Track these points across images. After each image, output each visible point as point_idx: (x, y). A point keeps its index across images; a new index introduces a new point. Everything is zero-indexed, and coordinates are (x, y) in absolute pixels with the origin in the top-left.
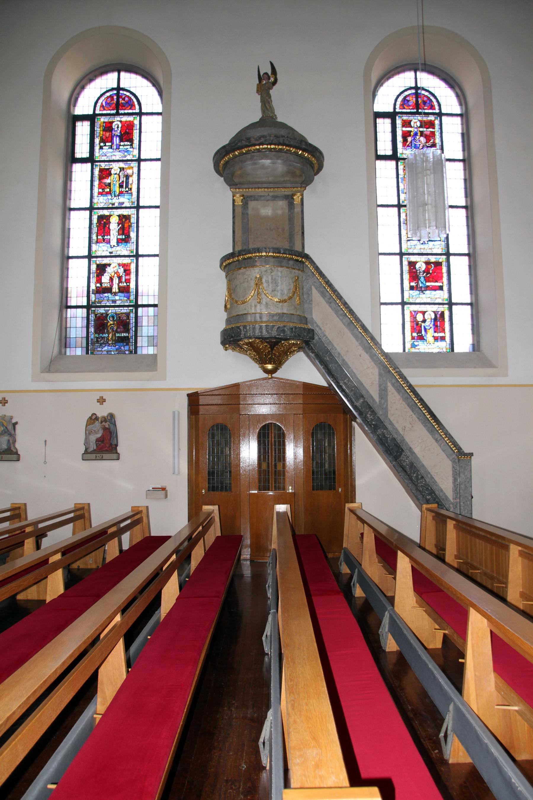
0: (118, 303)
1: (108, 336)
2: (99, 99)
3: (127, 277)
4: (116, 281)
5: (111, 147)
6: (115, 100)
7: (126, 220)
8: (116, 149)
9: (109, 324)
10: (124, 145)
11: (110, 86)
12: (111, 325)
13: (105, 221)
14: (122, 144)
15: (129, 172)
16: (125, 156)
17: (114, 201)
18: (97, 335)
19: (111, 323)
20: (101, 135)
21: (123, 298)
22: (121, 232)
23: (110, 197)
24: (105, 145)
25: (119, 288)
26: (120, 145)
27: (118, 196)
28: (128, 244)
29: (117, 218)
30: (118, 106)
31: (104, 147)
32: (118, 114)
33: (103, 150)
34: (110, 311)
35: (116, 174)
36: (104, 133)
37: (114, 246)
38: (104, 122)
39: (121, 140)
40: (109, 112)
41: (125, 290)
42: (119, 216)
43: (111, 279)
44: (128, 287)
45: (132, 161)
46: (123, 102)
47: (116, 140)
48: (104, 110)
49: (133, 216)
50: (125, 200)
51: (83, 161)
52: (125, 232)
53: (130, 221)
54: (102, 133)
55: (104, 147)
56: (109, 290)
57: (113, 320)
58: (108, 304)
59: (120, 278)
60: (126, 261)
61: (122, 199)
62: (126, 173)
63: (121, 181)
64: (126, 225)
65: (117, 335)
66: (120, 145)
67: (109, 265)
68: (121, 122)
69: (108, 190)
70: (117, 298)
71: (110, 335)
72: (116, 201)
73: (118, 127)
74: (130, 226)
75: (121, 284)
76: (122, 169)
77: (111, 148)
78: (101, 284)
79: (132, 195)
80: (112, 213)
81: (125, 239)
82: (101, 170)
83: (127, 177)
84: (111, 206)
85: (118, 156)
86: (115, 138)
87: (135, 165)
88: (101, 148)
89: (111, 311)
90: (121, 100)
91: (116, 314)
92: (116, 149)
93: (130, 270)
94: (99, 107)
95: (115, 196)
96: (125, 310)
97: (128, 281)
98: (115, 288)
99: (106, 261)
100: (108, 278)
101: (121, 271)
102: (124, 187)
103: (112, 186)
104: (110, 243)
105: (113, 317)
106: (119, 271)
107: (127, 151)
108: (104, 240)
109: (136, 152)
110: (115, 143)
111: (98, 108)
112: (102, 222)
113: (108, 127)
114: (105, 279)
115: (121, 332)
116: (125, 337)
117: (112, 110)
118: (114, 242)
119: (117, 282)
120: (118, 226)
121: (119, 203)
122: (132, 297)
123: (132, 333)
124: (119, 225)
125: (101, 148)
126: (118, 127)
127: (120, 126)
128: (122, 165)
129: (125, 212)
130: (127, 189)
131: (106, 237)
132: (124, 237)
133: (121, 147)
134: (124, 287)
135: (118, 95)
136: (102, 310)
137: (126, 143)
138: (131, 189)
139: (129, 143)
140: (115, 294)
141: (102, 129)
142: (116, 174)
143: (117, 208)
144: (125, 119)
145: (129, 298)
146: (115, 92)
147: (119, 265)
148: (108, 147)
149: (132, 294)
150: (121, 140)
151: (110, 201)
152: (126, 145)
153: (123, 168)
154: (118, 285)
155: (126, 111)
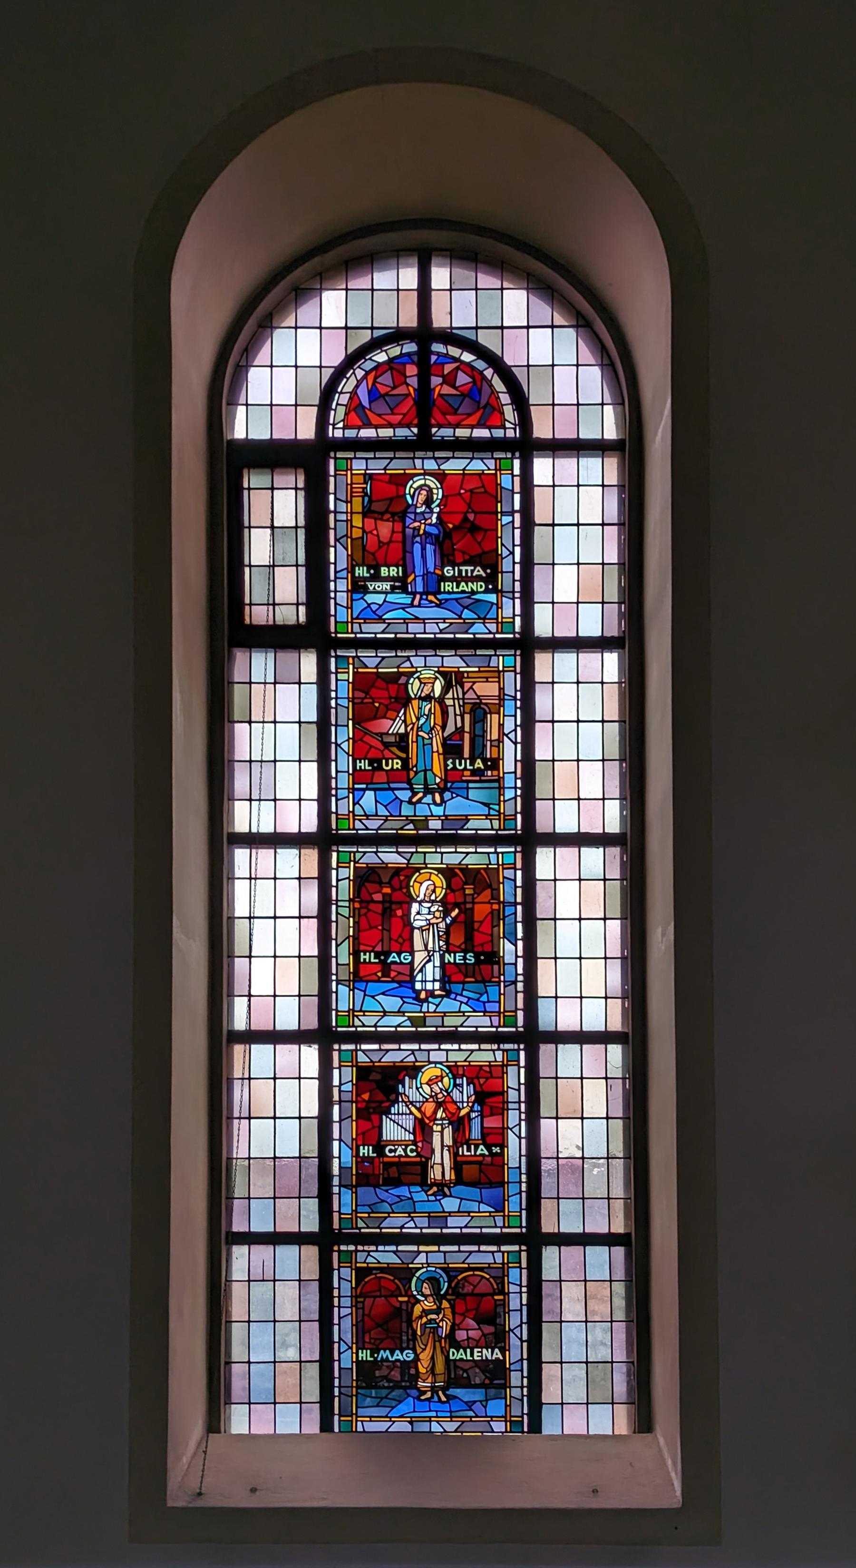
0: (455, 1225)
1: (417, 1359)
2: (340, 373)
3: (492, 1123)
4: (442, 1137)
5: (401, 585)
6: (414, 382)
7: (478, 892)
8: (426, 593)
9: (417, 1310)
10: (452, 579)
11: (386, 319)
12: (425, 1312)
13: (387, 890)
14: (448, 571)
15: (487, 689)
16: (468, 626)
17: (422, 810)
18: (365, 1355)
19: (429, 1304)
20: (357, 533)
21: (474, 1206)
22: (458, 939)
23: (404, 795)
24: (376, 577)
25: (457, 1166)
26: (443, 578)
27: (442, 791)
28: (492, 990)
29: (439, 881)
30: (425, 408)
31: (371, 586)
32: (424, 443)
33: (370, 598)
34: (422, 1258)
35: (428, 698)
36: (370, 522)
37: (431, 994)
38: (369, 477)
39: (446, 558)
40: (386, 433)
41: (482, 1174)
42: (448, 873)
43: (423, 1129)
44: (498, 1161)
45: (495, 644)
46: (447, 390)
47: (424, 558)
48: (368, 425)
49: (509, 873)
50: (470, 807)
51: (279, 638)
52: (478, 938)
53: (495, 897)
54: (358, 521)
55: (371, 586)
56: (414, 1171)
57: (437, 1296)
58: (410, 1229)
59: (459, 1124)
60: (485, 1055)
61: (456, 806)
62: (470, 695)
63: (450, 729)
64: (481, 911)
65: (456, 1355)
66: (443, 578)
67: (414, 1071)
68: (441, 477)
69: (397, 764)
70: (450, 1204)
71: (425, 1357)
72: (434, 813)
73: (428, 502)
74: (496, 917)
75: (464, 1151)
76: (452, 679)
77: (404, 590)
78: (379, 1147)
79: (501, 789)
80: (417, 860)
81: (475, 962)
82: (364, 683)
83: (479, 711)
84: (410, 829)
85: (433, 622)
86: (417, 548)
87: (510, 661)
88: (358, 588)
89: (426, 1258)
90: (435, 381)
91: (446, 1270)
92: (426, 593)
93: (503, 1093)
94: (341, 411)
95: (427, 791)
96: (485, 1256)
97: (495, 1138)
98: (441, 1165)
99: (396, 1054)
100: (409, 1123)
101: (464, 1094)
102: (466, 754)
103: (413, 748)
104: (412, 981)
105: (434, 1281)
106: (456, 1095)
107: (471, 602)
108: (386, 968)
109: (511, 608)
110: (419, 570)
111: (337, 414)
112: (378, 897)
113: (385, 500)
114: (396, 1129)
115: (471, 1345)
116: (483, 1365)
117: (400, 425)
118: (429, 976)
119: (448, 1141)
120: (446, 913)
121: (446, 818)
122: (516, 1204)
123: (517, 1350)
124: (446, 906)
125: (358, 588)
126: (428, 502)
127: (438, 494)
128: (453, 661)
129: (474, 858)
130: (479, 764)
131: (393, 958)
132: (471, 958)
133: (448, 586)
134: (479, 1162)
135: (423, 358)
136: (385, 1255)
137: (466, 569)
138: (495, 764)
139: (479, 571)
140: (442, 1188)
141: (358, 507)
142: (428, 698)
143: (437, 840)
144: (454, 465)
145: (499, 1207)
146: (410, 347)
147: (454, 1070)
148: (386, 586)
149: (513, 1189)
150: (446, 558)
151: (407, 810)
152: (467, 579)
153: (459, 675)
154: (455, 1155)
155: (462, 433)
